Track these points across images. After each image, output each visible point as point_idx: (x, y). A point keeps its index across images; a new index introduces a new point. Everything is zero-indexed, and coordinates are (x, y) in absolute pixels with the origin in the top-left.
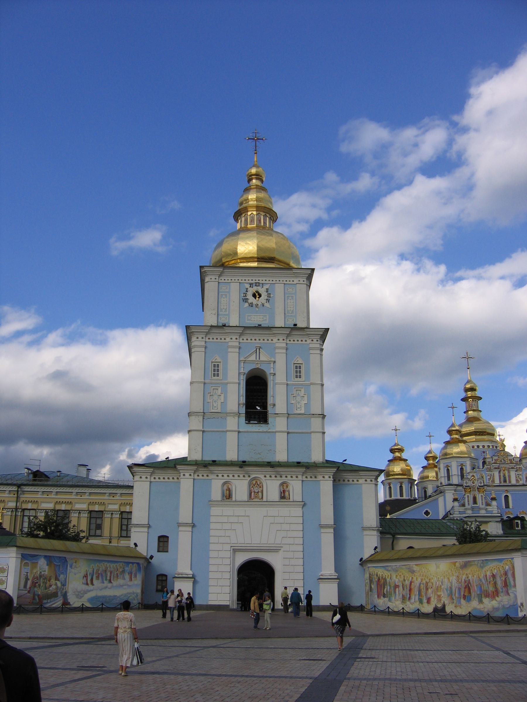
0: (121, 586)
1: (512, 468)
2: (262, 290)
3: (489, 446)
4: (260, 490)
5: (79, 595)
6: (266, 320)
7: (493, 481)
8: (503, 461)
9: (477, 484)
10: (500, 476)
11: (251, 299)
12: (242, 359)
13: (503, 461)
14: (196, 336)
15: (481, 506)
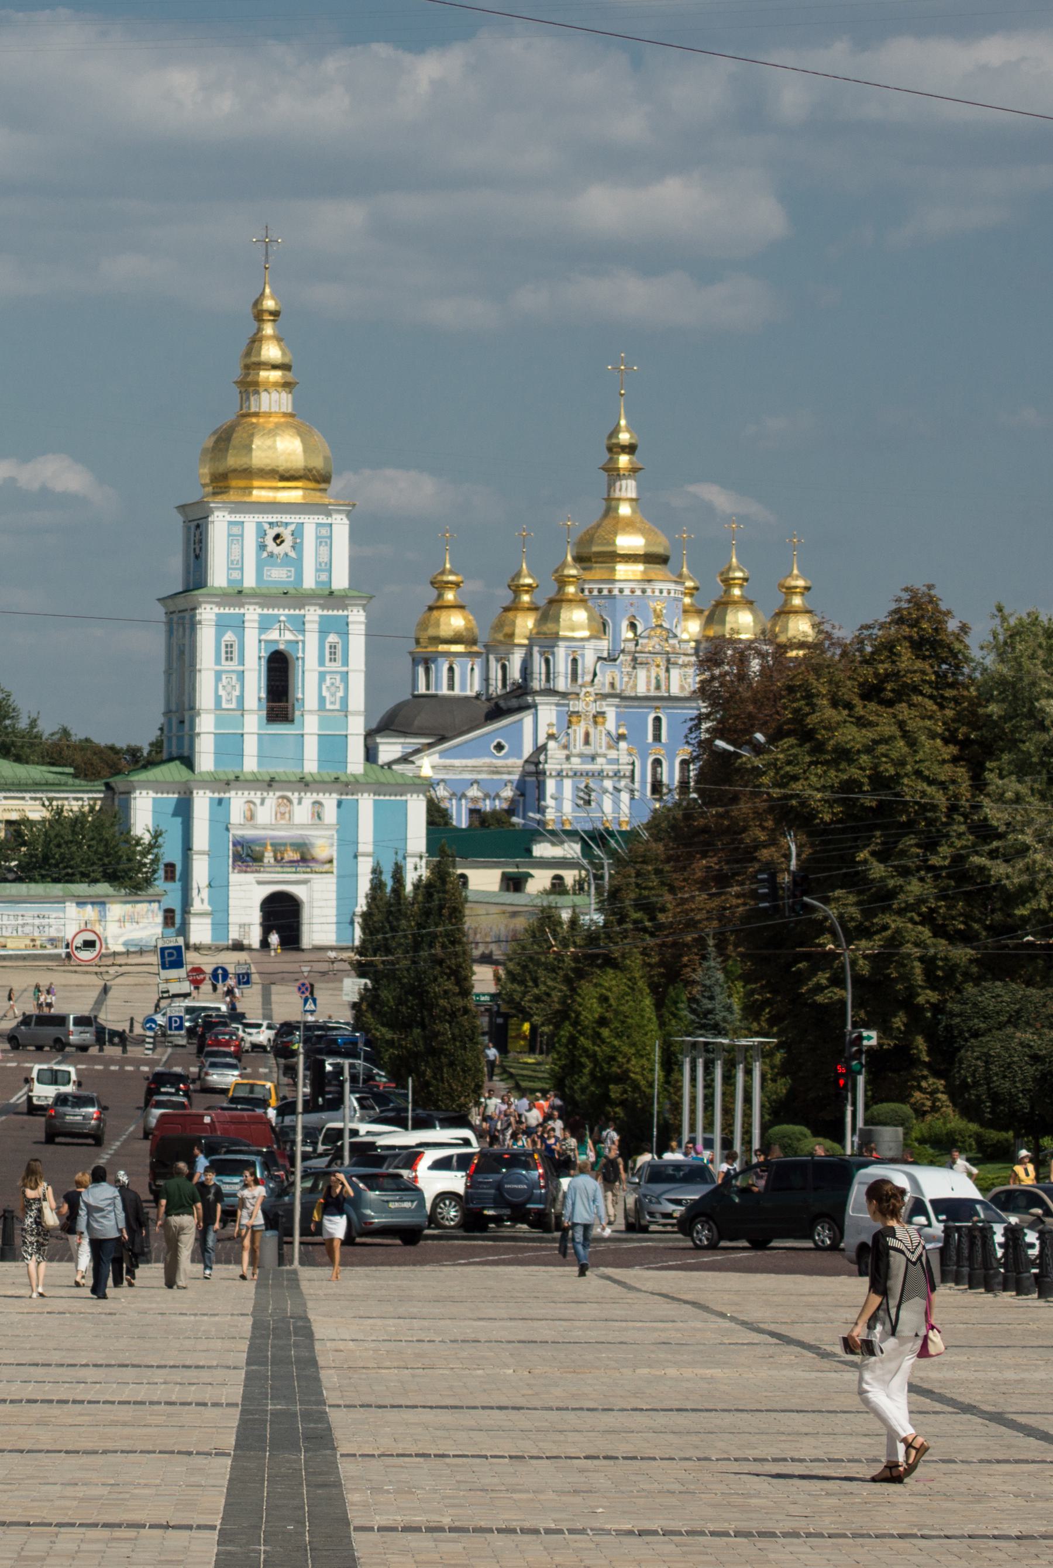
0: (145, 928)
1: (675, 664)
2: (286, 533)
3: (644, 591)
4: (287, 810)
5: (116, 937)
6: (290, 577)
7: (635, 686)
8: (657, 647)
9: (593, 709)
10: (648, 677)
11: (271, 546)
12: (263, 637)
13: (657, 647)
14: (203, 606)
15: (600, 751)
